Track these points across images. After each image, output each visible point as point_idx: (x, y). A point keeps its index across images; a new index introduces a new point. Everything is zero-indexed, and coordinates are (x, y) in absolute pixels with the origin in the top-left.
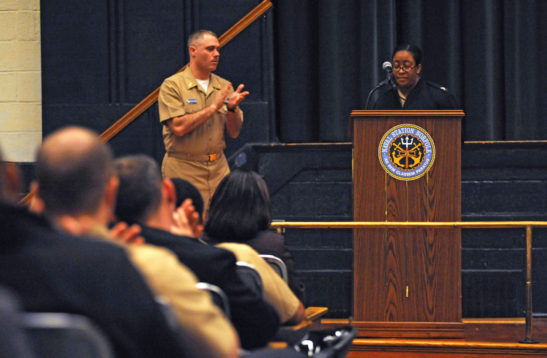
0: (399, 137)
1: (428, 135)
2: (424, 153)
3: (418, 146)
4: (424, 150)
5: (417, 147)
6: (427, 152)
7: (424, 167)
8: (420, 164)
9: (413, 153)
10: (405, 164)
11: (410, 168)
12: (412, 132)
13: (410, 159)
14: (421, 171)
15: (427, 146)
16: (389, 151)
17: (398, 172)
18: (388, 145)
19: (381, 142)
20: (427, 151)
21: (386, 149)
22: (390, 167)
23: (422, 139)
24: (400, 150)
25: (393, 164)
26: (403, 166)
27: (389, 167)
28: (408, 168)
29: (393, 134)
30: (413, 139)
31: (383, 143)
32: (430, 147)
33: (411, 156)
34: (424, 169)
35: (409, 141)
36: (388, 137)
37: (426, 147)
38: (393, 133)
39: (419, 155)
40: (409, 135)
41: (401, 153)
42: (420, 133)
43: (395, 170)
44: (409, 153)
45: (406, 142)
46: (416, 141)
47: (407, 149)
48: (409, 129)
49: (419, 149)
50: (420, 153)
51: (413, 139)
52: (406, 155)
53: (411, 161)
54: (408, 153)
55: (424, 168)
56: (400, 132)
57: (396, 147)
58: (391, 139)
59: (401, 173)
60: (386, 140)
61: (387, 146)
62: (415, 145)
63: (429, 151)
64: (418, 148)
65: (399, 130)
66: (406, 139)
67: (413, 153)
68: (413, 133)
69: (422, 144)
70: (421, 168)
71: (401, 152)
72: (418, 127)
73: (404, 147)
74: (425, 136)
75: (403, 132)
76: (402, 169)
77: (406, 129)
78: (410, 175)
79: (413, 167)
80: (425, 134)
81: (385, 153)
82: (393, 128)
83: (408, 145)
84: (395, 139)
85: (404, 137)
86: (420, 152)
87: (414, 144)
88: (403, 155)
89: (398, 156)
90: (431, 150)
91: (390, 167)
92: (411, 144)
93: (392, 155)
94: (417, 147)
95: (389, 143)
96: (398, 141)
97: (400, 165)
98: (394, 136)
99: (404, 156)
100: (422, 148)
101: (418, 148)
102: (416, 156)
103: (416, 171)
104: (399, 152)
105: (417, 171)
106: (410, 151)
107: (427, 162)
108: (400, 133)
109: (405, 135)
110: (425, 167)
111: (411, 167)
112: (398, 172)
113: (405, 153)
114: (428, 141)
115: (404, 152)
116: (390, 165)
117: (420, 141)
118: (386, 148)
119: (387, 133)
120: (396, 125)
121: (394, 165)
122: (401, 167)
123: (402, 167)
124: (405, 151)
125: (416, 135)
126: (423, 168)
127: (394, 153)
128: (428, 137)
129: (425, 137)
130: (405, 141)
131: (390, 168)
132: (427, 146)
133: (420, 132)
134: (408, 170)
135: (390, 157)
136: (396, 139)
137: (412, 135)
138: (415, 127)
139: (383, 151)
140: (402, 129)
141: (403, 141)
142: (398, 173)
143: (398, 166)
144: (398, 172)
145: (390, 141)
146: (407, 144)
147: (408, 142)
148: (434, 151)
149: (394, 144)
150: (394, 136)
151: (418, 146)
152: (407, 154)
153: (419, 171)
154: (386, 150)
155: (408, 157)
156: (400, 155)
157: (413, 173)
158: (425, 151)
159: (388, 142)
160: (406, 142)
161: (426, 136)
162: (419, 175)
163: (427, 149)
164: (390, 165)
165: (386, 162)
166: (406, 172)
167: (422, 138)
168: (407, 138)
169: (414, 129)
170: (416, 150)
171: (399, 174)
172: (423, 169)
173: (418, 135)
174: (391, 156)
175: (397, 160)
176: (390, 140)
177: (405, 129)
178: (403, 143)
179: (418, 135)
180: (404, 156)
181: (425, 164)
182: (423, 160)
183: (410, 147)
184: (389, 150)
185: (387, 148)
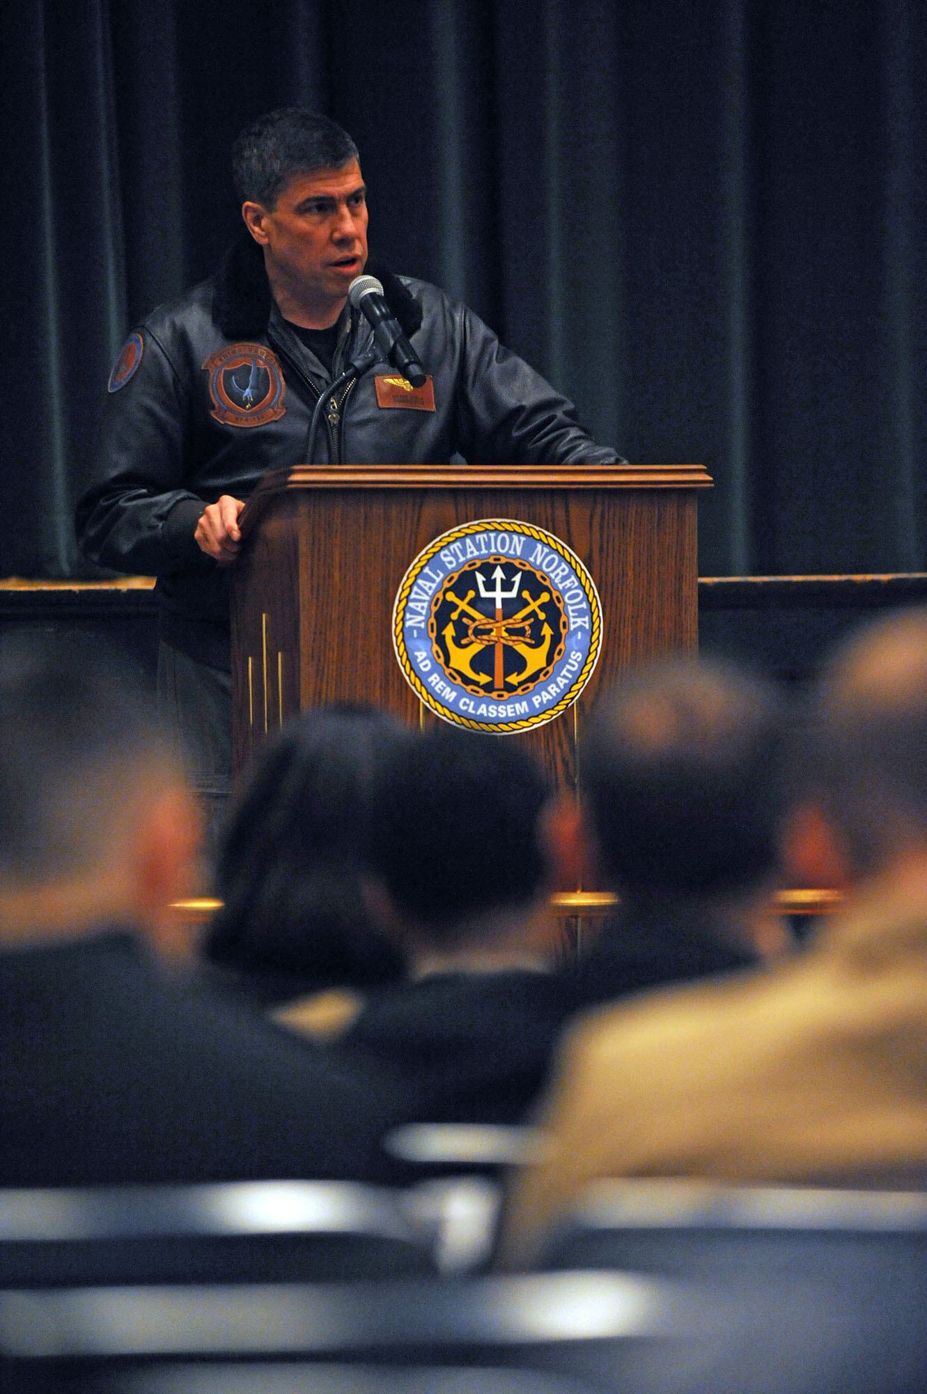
0: (466, 568)
1: (576, 562)
4: (563, 619)
5: (534, 606)
6: (572, 627)
7: (562, 682)
8: (547, 672)
9: (521, 632)
10: (490, 673)
12: (515, 550)
13: (509, 652)
14: (551, 698)
15: (572, 605)
16: (432, 625)
17: (468, 701)
18: (427, 598)
19: (400, 590)
20: (574, 623)
21: (420, 614)
22: (437, 683)
23: (552, 576)
24: (474, 620)
26: (484, 679)
27: (433, 684)
29: (445, 559)
32: (584, 605)
33: (513, 641)
34: (562, 690)
35: (507, 586)
36: (427, 570)
37: (570, 608)
39: (544, 636)
40: (507, 563)
41: (478, 632)
42: (547, 555)
44: (507, 630)
45: (494, 590)
46: (534, 584)
47: (499, 615)
49: (542, 616)
50: (547, 631)
52: (496, 639)
53: (515, 662)
54: (504, 628)
56: (473, 548)
57: (457, 606)
58: (438, 575)
59: (476, 708)
61: (425, 605)
62: (530, 600)
63: (580, 621)
64: (538, 611)
66: (493, 577)
67: (521, 632)
68: (519, 554)
70: (549, 689)
71: (476, 627)
72: (538, 528)
73: (485, 606)
74: (564, 565)
75: (484, 551)
77: (496, 538)
78: (510, 715)
79: (520, 684)
81: (419, 629)
82: (446, 534)
83: (503, 600)
84: (452, 578)
87: (526, 594)
88: (485, 637)
89: (464, 642)
90: (587, 619)
91: (437, 683)
92: (513, 594)
93: (444, 636)
94: (534, 606)
95: (430, 592)
96: (464, 583)
97: (471, 675)
98: (450, 566)
99: (489, 641)
100: (553, 612)
101: (538, 611)
102: (533, 642)
103: (534, 699)
105: (536, 701)
106: (511, 621)
107: (573, 666)
108: (472, 553)
109: (491, 561)
110: (567, 681)
111: (516, 684)
112: (465, 704)
113: (491, 630)
114: (577, 584)
115: (488, 627)
118: (419, 609)
119: (423, 552)
120: (458, 525)
121: (450, 674)
122: (476, 683)
123: (481, 684)
124: (492, 621)
125: (532, 559)
127: (449, 632)
128: (575, 570)
129: (563, 570)
130: (490, 586)
131: (436, 689)
132: (572, 605)
134: (505, 693)
135: (436, 647)
137: (516, 563)
138: (527, 532)
139: (408, 624)
140: (477, 537)
141: (484, 582)
142: (465, 708)
143: (467, 680)
144: (468, 701)
145: (434, 586)
147: (503, 590)
148: (600, 624)
149: (451, 597)
150: (450, 566)
152: (499, 633)
155: (504, 645)
156: (473, 638)
158: (564, 623)
159: (426, 588)
160: (494, 590)
162: (544, 713)
164: (435, 675)
167: (552, 572)
168: (499, 574)
169: (523, 539)
170: (532, 620)
171: (471, 710)
172: (558, 691)
175: (461, 659)
176: (433, 581)
177: (489, 538)
180: (486, 643)
181: (564, 672)
183: (511, 607)
184: (433, 620)
185: (424, 612)
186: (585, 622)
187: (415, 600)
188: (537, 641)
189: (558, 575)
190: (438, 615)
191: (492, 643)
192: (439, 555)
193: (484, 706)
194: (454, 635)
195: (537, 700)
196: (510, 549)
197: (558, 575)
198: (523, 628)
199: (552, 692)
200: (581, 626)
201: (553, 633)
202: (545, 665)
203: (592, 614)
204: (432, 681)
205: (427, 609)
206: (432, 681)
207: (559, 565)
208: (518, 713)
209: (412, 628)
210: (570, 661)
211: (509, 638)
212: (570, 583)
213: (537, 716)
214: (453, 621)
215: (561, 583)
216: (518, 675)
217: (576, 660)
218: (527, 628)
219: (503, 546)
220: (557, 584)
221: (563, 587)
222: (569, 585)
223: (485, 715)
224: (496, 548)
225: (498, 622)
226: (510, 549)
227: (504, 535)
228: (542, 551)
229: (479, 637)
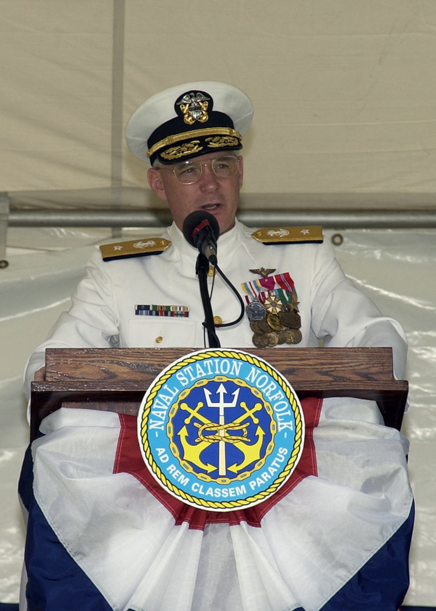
2: (273, 432)
3: (254, 410)
4: (273, 423)
5: (250, 413)
6: (280, 429)
7: (272, 471)
9: (239, 433)
11: (230, 475)
12: (234, 372)
14: (264, 482)
15: (279, 413)
17: (198, 485)
18: (166, 408)
20: (281, 426)
21: (161, 420)
22: (174, 472)
23: (264, 391)
24: (203, 424)
25: (182, 462)
26: (210, 468)
27: (171, 472)
28: (225, 474)
29: (179, 379)
30: (238, 390)
31: (152, 404)
32: (289, 413)
36: (165, 387)
37: (278, 415)
38: (181, 373)
39: (258, 436)
41: (206, 433)
42: (259, 375)
43: (187, 480)
48: (225, 363)
49: (256, 421)
50: (260, 432)
51: (238, 390)
55: (272, 474)
56: (202, 371)
58: (175, 391)
59: (205, 490)
60: (160, 395)
61: (165, 413)
63: (286, 425)
65: (198, 365)
66: (217, 392)
67: (239, 433)
68: (237, 374)
69: (266, 404)
70: (262, 475)
71: (204, 429)
74: (272, 383)
75: (210, 373)
76: (209, 479)
77: (219, 363)
78: (231, 495)
79: (240, 472)
80: (273, 377)
81: (159, 430)
83: (225, 409)
85: (213, 386)
86: (259, 427)
87: (243, 405)
88: (211, 437)
90: (291, 423)
91: (174, 472)
92: (233, 404)
93: (179, 436)
94: (250, 413)
95: (169, 404)
98: (184, 384)
99: (214, 440)
102: (249, 440)
103: (250, 483)
104: (198, 429)
105: (252, 485)
106: (231, 425)
107: (281, 458)
110: (276, 470)
111: (236, 472)
112: (196, 487)
114: (283, 397)
116: (172, 466)
117: (259, 396)
118: (160, 416)
122: (205, 472)
123: (208, 472)
124: (216, 425)
126: (269, 474)
127: (183, 433)
129: (272, 387)
131: (173, 475)
132: (279, 413)
133: (259, 372)
136: (188, 392)
137: (236, 381)
139: (151, 427)
140: (205, 362)
142: (196, 490)
143: (197, 470)
144: (198, 485)
145: (171, 399)
146: (222, 405)
147: (225, 401)
150: (184, 384)
151: (254, 410)
153: (260, 482)
154: (162, 423)
155: (226, 442)
156: (202, 437)
157: (241, 490)
159: (165, 401)
161: (278, 382)
162: (258, 494)
163: (279, 419)
164: (172, 466)
165: (161, 458)
166: (221, 486)
168: (222, 390)
169: (241, 363)
170: (248, 424)
171: (200, 492)
172: (270, 477)
173: (253, 381)
174: (177, 439)
177: (214, 363)
178: (210, 404)
179: (253, 381)
181: (274, 463)
182: (268, 452)
184: (170, 425)
185: (164, 418)
186: (290, 425)
187: (157, 409)
188: (253, 440)
189: (268, 390)
190: (174, 420)
191: (216, 441)
192: (176, 375)
193: (210, 489)
194: (187, 435)
195: (253, 484)
196: (230, 371)
197: (268, 390)
198: (242, 429)
199: (265, 478)
200: (287, 428)
201: (264, 434)
202: (259, 458)
203: (296, 419)
204: (170, 470)
205: (166, 416)
206: (170, 470)
207: (269, 383)
208: (238, 494)
209: (154, 430)
210: (278, 455)
211: (229, 438)
212: (278, 396)
213: (253, 497)
214: (187, 425)
215: (270, 396)
216: (237, 466)
217: (282, 454)
218: (244, 430)
219: (225, 369)
220: (267, 397)
221: (273, 399)
222: (277, 398)
223: (212, 495)
224: (219, 370)
225: (221, 425)
226: (230, 371)
227: (225, 360)
228: (256, 372)
229: (207, 437)
